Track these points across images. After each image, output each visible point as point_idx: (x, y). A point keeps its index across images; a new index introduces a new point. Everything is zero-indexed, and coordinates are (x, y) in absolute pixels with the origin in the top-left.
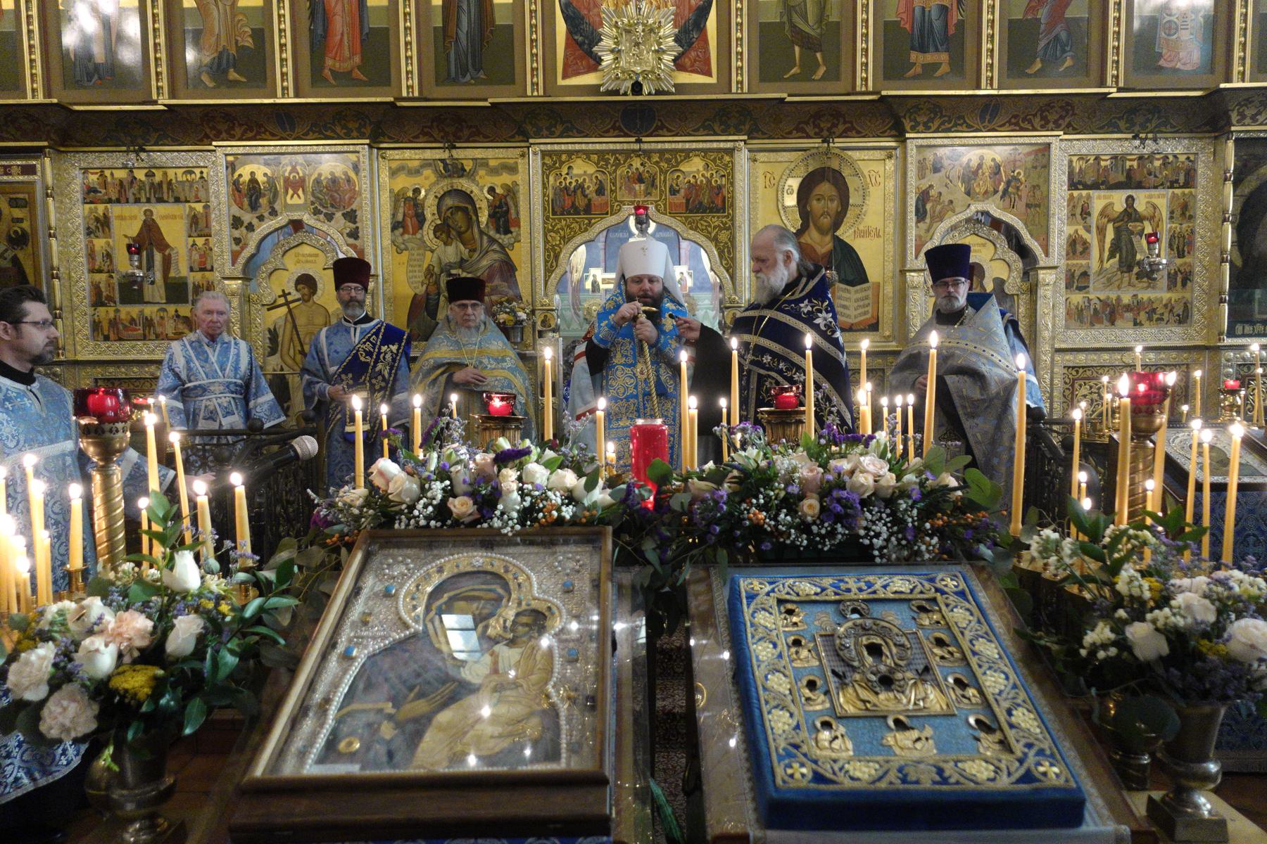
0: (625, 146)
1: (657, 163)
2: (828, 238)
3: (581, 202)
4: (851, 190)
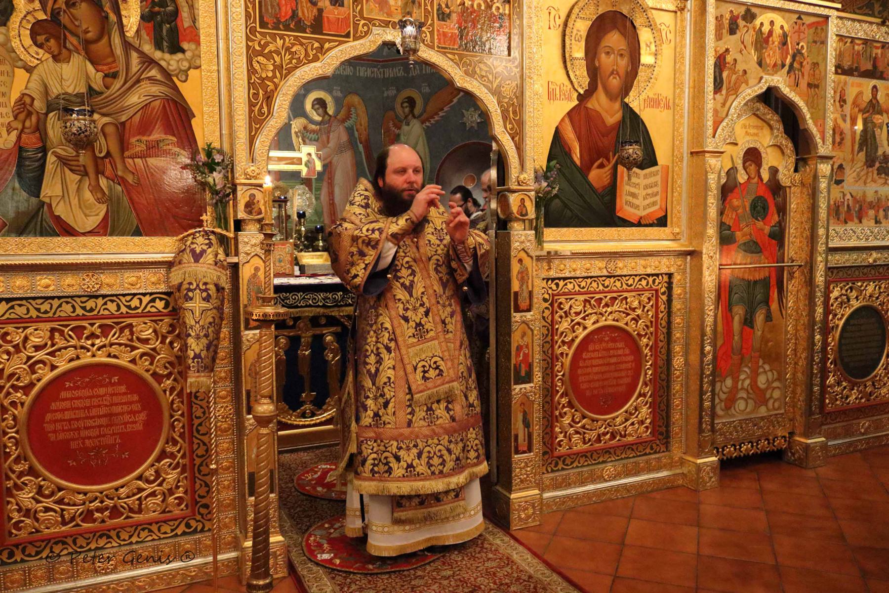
2: (617, 105)
4: (643, 45)
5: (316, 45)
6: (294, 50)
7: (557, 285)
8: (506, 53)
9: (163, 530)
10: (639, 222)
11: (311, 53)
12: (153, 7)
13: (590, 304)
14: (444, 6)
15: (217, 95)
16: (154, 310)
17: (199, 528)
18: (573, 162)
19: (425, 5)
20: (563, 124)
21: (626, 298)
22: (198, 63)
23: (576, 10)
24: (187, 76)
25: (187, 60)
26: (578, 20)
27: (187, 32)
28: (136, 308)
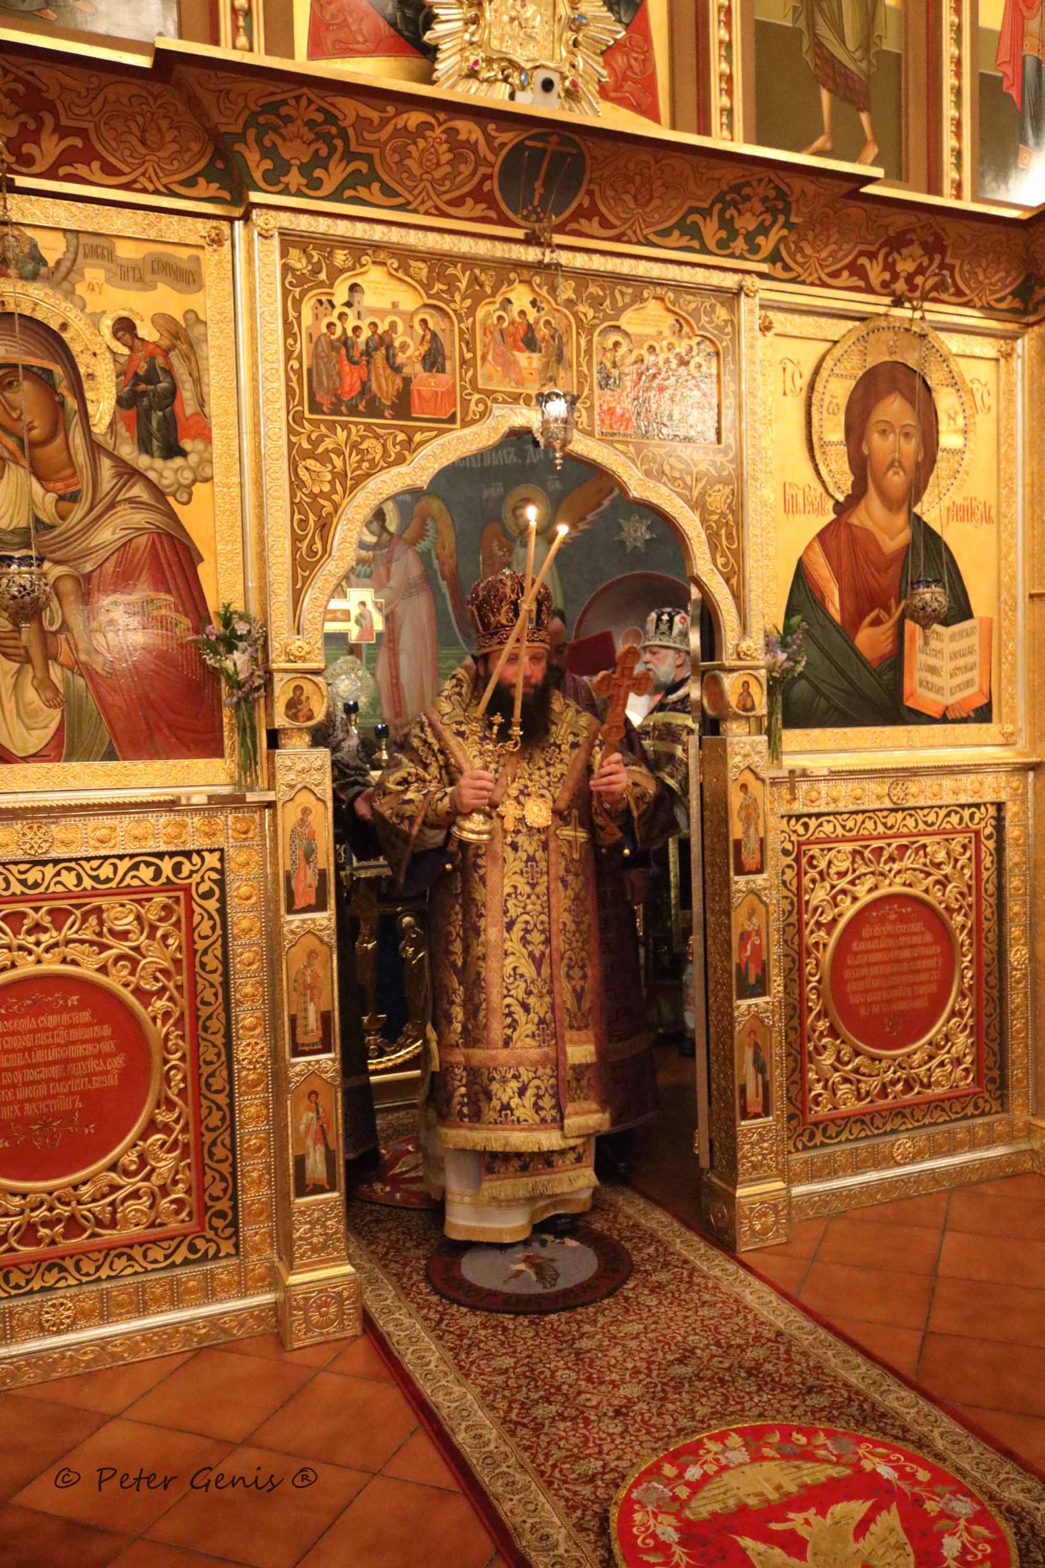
0: (500, 250)
1: (570, 303)
2: (901, 519)
3: (385, 386)
4: (942, 417)
5: (401, 437)
6: (364, 446)
7: (806, 826)
8: (712, 436)
9: (151, 1255)
10: (944, 715)
11: (393, 451)
12: (135, 384)
13: (863, 858)
14: (609, 365)
15: (239, 523)
16: (136, 883)
17: (211, 1253)
18: (831, 620)
19: (579, 365)
20: (810, 553)
21: (924, 846)
22: (208, 472)
23: (828, 363)
24: (190, 495)
25: (191, 468)
26: (833, 379)
27: (191, 422)
28: (108, 880)
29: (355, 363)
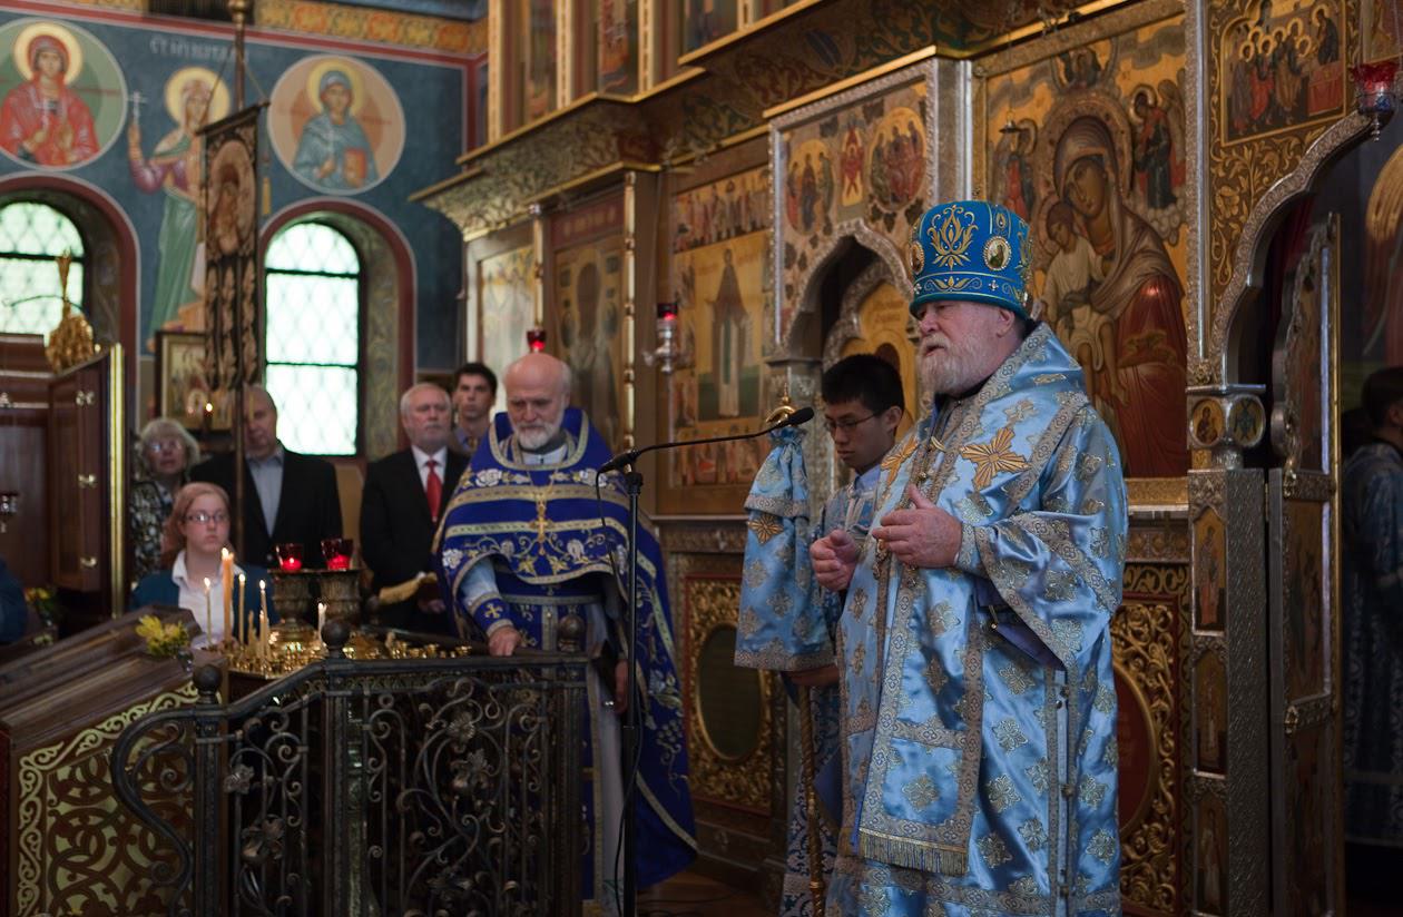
12: (1148, 148)
29: (1264, 79)
